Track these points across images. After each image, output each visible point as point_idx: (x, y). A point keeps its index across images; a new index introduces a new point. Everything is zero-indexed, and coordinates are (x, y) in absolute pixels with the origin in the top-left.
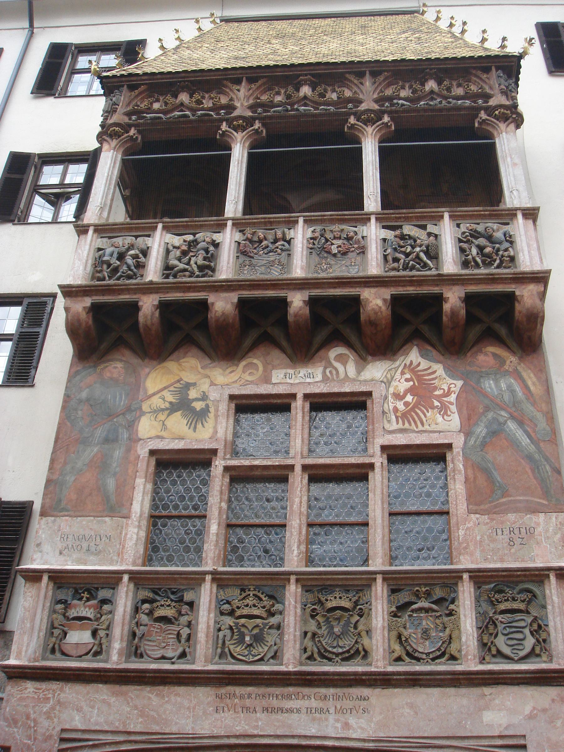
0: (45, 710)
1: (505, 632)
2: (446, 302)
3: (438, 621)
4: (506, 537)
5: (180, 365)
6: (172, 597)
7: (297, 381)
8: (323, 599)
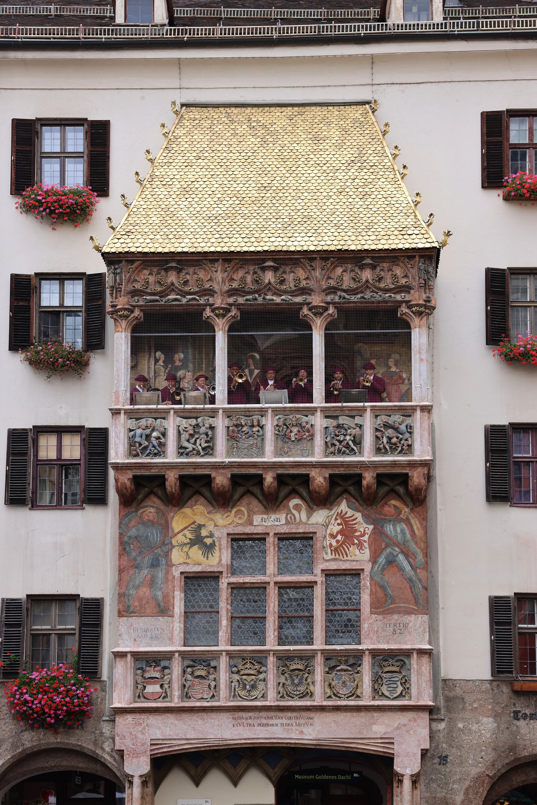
0: (140, 729)
1: (387, 684)
2: (364, 479)
3: (351, 677)
4: (392, 629)
5: (193, 511)
6: (204, 664)
7: (269, 524)
8: (288, 664)
